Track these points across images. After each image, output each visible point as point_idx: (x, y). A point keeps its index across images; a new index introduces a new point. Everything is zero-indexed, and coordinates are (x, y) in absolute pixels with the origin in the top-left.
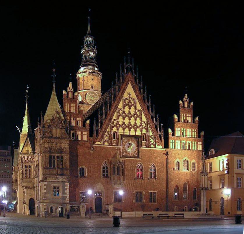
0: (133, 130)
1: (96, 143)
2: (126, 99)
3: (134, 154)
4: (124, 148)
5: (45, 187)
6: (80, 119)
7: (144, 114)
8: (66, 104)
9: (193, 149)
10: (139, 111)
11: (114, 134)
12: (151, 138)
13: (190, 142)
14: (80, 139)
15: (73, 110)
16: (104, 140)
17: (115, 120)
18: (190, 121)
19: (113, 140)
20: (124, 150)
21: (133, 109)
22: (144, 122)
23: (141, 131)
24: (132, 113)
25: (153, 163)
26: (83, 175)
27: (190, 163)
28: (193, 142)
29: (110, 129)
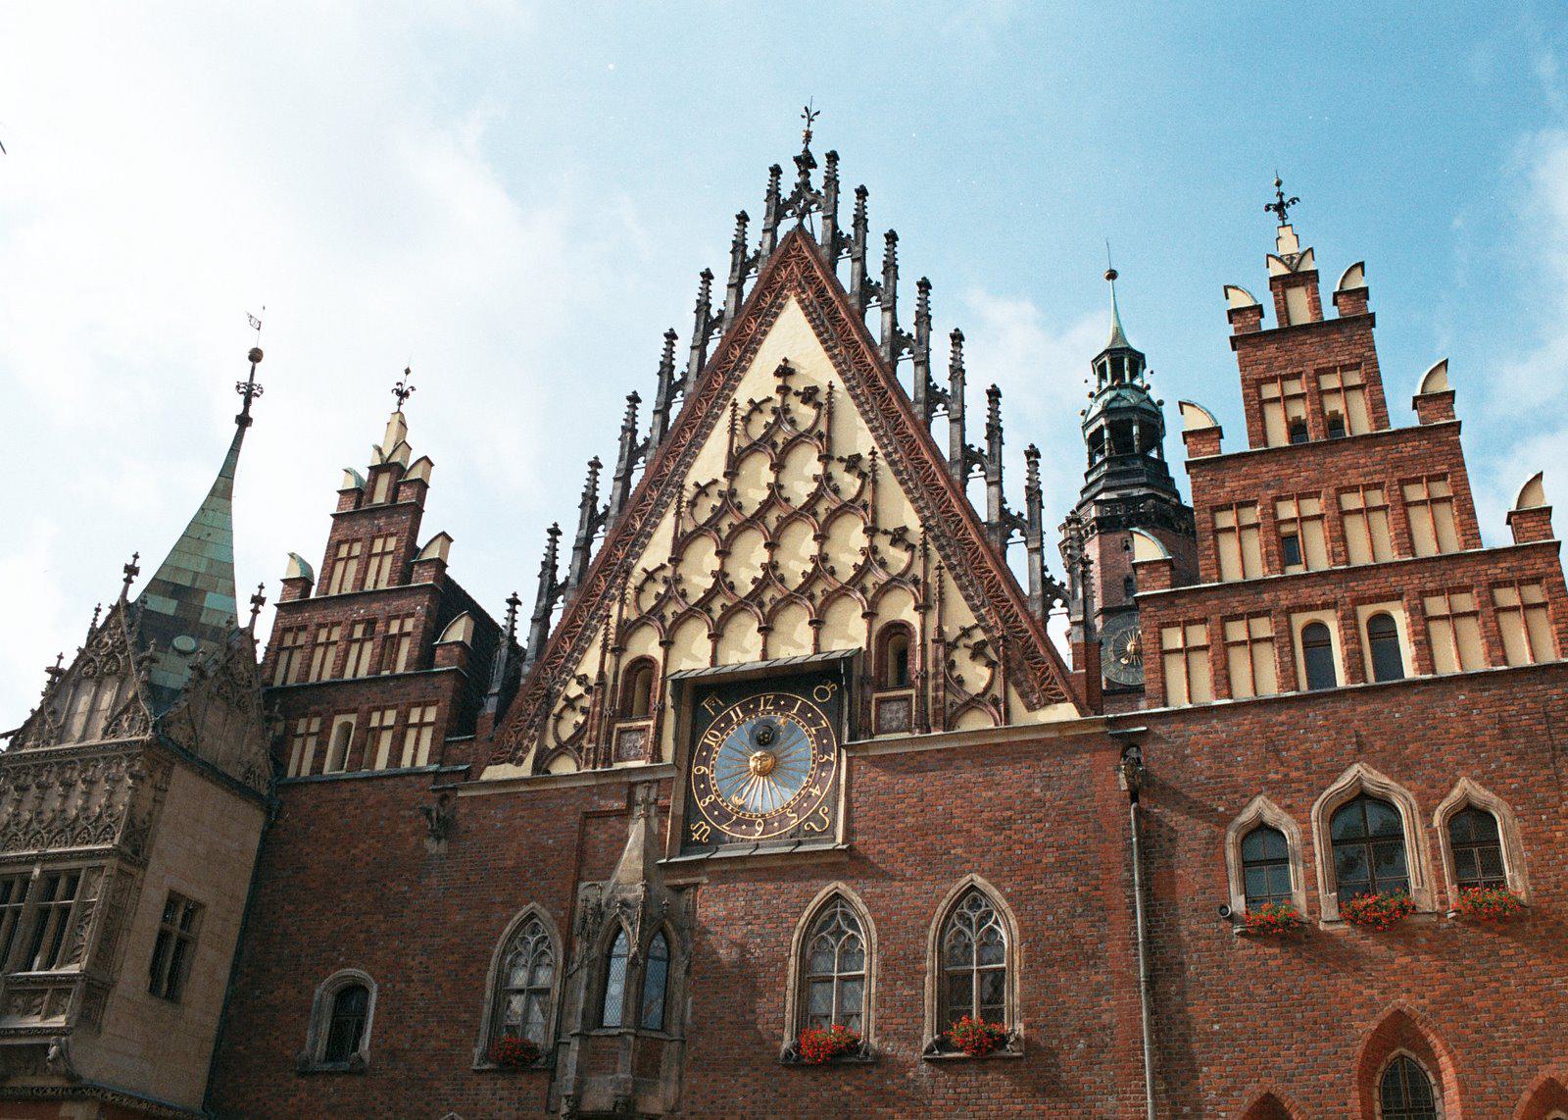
1: (484, 777)
3: (794, 822)
4: (703, 778)
7: (897, 473)
8: (343, 552)
9: (1448, 664)
12: (961, 657)
14: (381, 764)
16: (551, 744)
18: (1361, 423)
19: (618, 725)
20: (707, 792)
22: (899, 537)
23: (870, 615)
25: (979, 881)
27: (1427, 814)
29: (604, 647)
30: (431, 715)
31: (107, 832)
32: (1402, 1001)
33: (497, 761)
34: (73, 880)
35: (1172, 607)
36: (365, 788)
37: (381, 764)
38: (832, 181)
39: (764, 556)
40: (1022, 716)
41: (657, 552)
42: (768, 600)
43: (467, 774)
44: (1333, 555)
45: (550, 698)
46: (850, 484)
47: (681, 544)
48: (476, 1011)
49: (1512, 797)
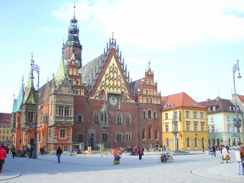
0: (115, 89)
2: (111, 67)
5: (55, 130)
6: (79, 80)
8: (70, 69)
9: (155, 103)
10: (119, 76)
11: (102, 91)
12: (127, 95)
13: (152, 98)
15: (75, 74)
17: (103, 82)
21: (115, 74)
22: (123, 84)
23: (121, 90)
24: (115, 77)
26: (81, 121)
28: (154, 99)
30: (83, 90)
31: (72, 103)
32: (151, 124)
33: (91, 96)
34: (68, 108)
35: (140, 95)
36: (79, 97)
37: (79, 94)
38: (115, 43)
39: (113, 83)
40: (131, 101)
41: (103, 79)
42: (113, 87)
43: (88, 97)
44: (150, 94)
45: (95, 91)
46: (119, 78)
47: (106, 79)
48: (93, 119)
49: (157, 112)
